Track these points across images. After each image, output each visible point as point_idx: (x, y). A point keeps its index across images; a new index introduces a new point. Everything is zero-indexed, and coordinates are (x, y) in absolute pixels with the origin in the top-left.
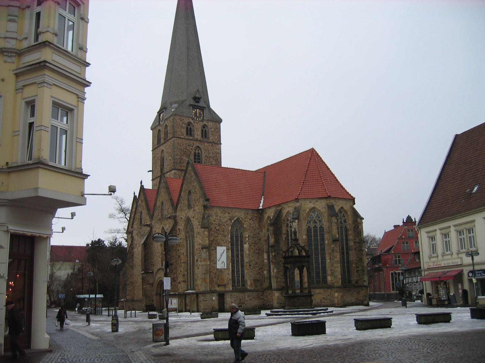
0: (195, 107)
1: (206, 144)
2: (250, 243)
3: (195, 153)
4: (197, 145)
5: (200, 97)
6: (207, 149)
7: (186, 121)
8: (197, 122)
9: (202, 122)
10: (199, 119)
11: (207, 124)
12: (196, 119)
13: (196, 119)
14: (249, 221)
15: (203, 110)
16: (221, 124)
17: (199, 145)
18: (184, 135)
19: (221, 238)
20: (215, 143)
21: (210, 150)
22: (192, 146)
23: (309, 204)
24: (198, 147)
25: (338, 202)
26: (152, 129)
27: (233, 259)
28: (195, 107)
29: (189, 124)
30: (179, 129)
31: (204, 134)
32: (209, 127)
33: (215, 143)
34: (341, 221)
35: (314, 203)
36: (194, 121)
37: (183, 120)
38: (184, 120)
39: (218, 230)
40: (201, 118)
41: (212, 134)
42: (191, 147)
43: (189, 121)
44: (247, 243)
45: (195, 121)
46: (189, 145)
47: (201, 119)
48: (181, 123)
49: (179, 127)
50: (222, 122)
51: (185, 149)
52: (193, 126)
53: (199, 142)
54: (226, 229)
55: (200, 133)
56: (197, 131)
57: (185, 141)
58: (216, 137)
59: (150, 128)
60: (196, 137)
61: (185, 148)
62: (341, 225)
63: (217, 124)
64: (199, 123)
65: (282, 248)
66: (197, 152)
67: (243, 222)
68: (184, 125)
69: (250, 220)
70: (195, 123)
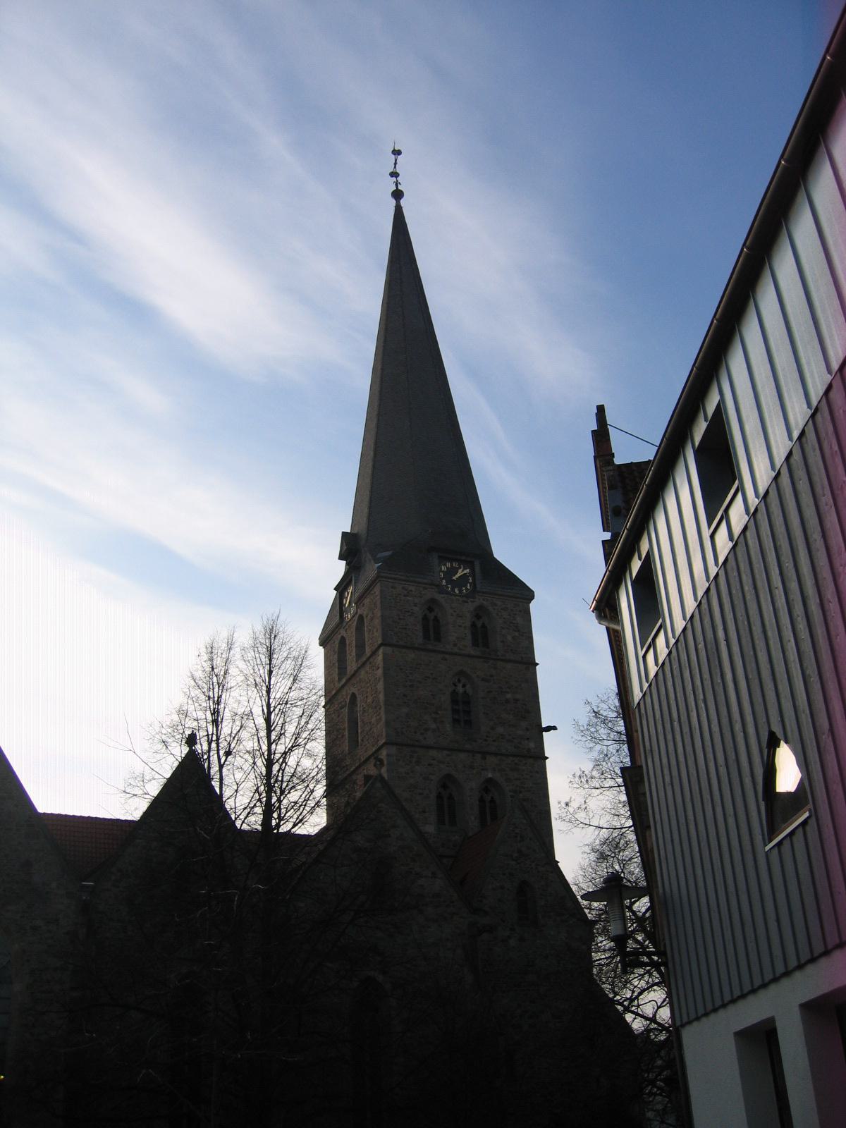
3: (454, 693)
10: (461, 591)
12: (453, 589)
13: (453, 589)
16: (533, 605)
24: (461, 673)
26: (320, 645)
29: (432, 605)
31: (481, 635)
47: (467, 589)
50: (533, 597)
59: (318, 641)
66: (460, 690)
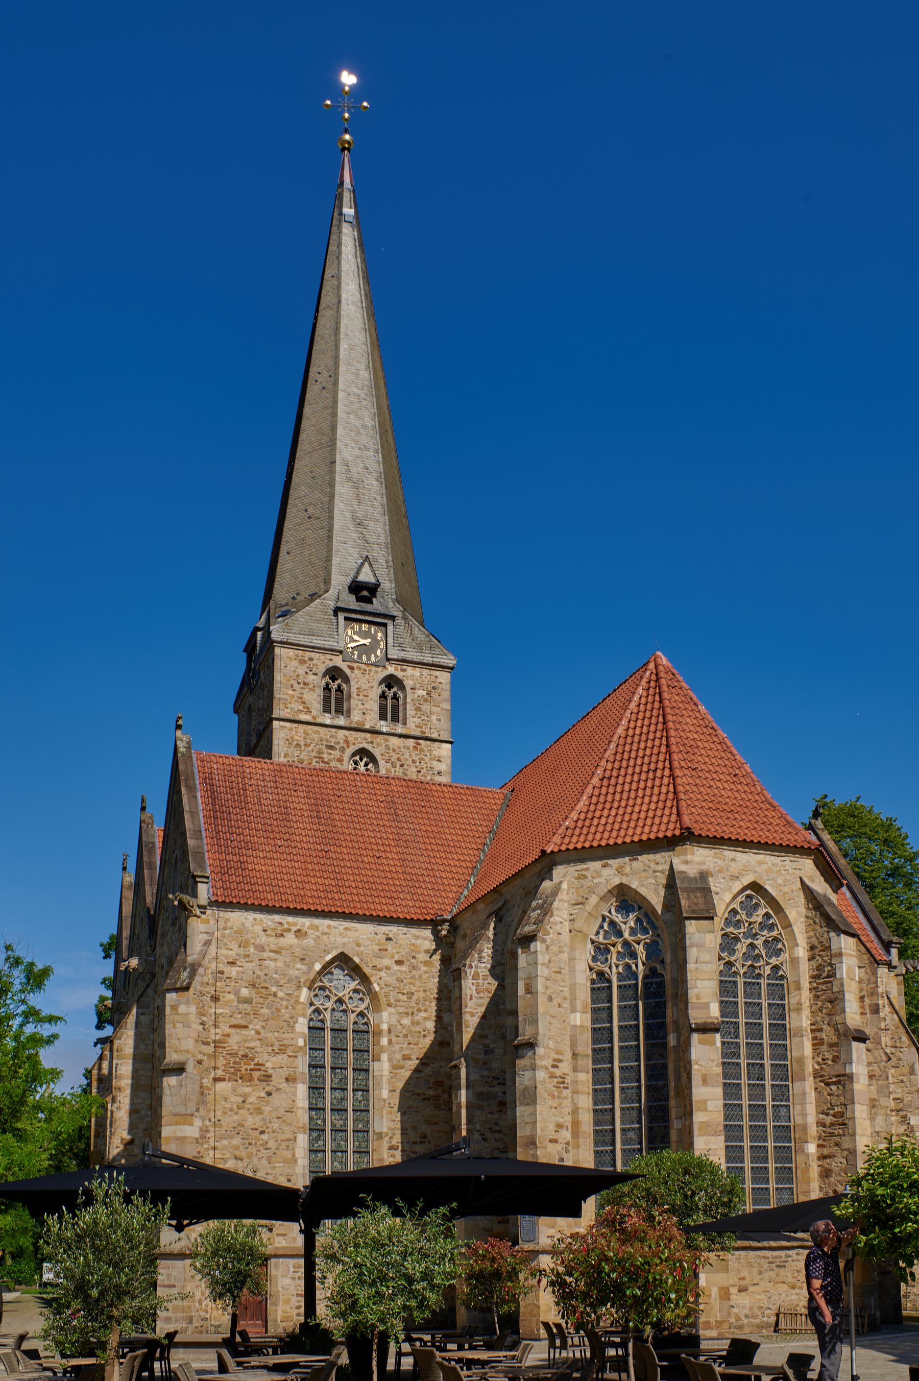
0: (353, 616)
1: (395, 741)
2: (398, 1056)
4: (361, 746)
5: (373, 580)
6: (399, 759)
7: (323, 662)
8: (363, 666)
9: (380, 669)
11: (399, 674)
12: (360, 657)
13: (360, 657)
14: (396, 968)
15: (385, 625)
17: (369, 747)
18: (314, 713)
19: (258, 1033)
20: (427, 739)
21: (410, 762)
22: (343, 750)
23: (599, 875)
25: (733, 860)
26: (236, 711)
27: (319, 1122)
28: (353, 616)
29: (334, 673)
30: (291, 692)
32: (408, 683)
33: (427, 739)
34: (752, 946)
35: (620, 871)
36: (350, 664)
37: (311, 659)
38: (315, 662)
39: (248, 1001)
40: (379, 653)
41: (418, 709)
42: (337, 753)
43: (331, 664)
44: (384, 1057)
45: (355, 665)
46: (331, 748)
47: (376, 656)
48: (302, 670)
49: (295, 685)
51: (315, 757)
52: (347, 680)
53: (368, 735)
54: (282, 999)
55: (374, 706)
56: (361, 697)
57: (315, 732)
58: (434, 717)
60: (356, 717)
61: (314, 754)
62: (750, 963)
63: (438, 673)
64: (370, 671)
65: (504, 1072)
67: (367, 970)
68: (314, 677)
69: (399, 963)
70: (356, 671)
